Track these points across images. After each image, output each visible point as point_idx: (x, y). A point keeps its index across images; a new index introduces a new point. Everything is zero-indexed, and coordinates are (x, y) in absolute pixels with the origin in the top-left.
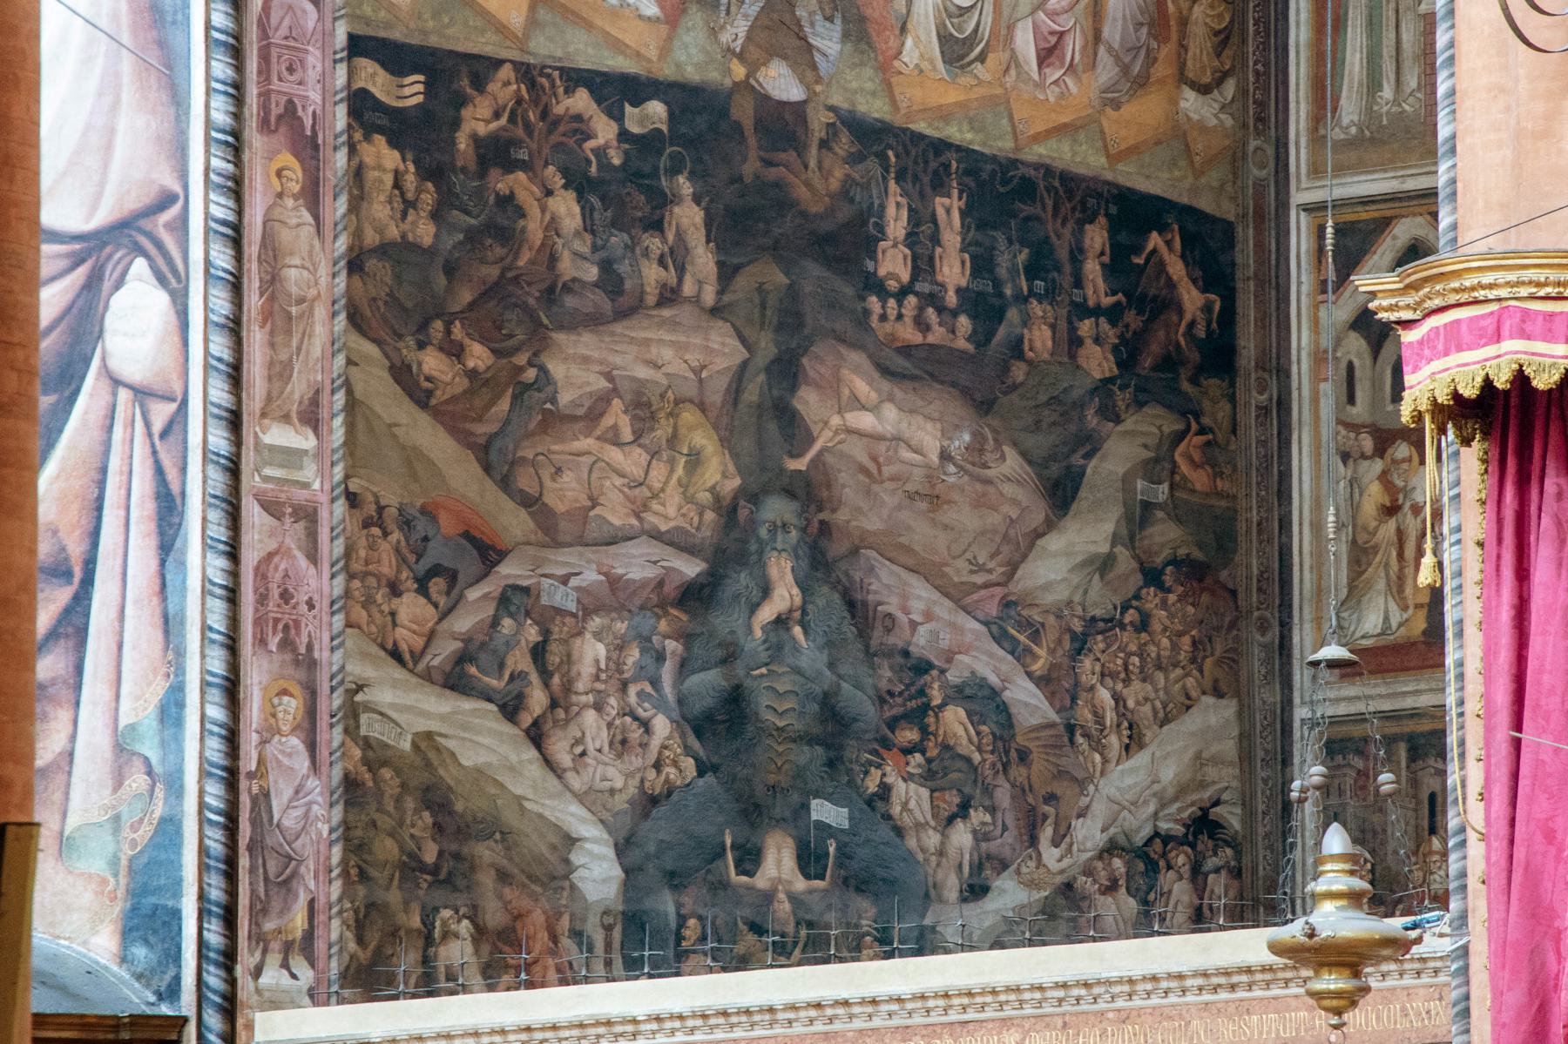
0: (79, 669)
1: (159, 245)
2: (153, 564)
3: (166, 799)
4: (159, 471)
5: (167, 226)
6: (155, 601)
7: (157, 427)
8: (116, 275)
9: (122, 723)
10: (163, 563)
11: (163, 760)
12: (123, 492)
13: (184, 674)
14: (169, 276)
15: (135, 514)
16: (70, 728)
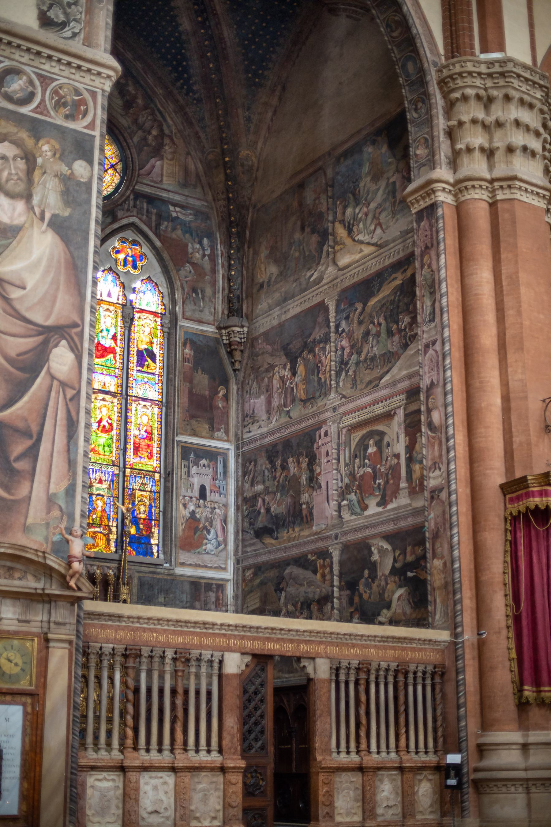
0: (34, 469)
1: (72, 339)
2: (65, 441)
3: (67, 522)
4: (68, 412)
5: (76, 334)
6: (65, 454)
7: (69, 396)
8: (55, 343)
9: (52, 491)
10: (69, 442)
11: (67, 508)
12: (54, 414)
13: (76, 480)
14: (75, 349)
15: (58, 423)
16: (29, 488)
